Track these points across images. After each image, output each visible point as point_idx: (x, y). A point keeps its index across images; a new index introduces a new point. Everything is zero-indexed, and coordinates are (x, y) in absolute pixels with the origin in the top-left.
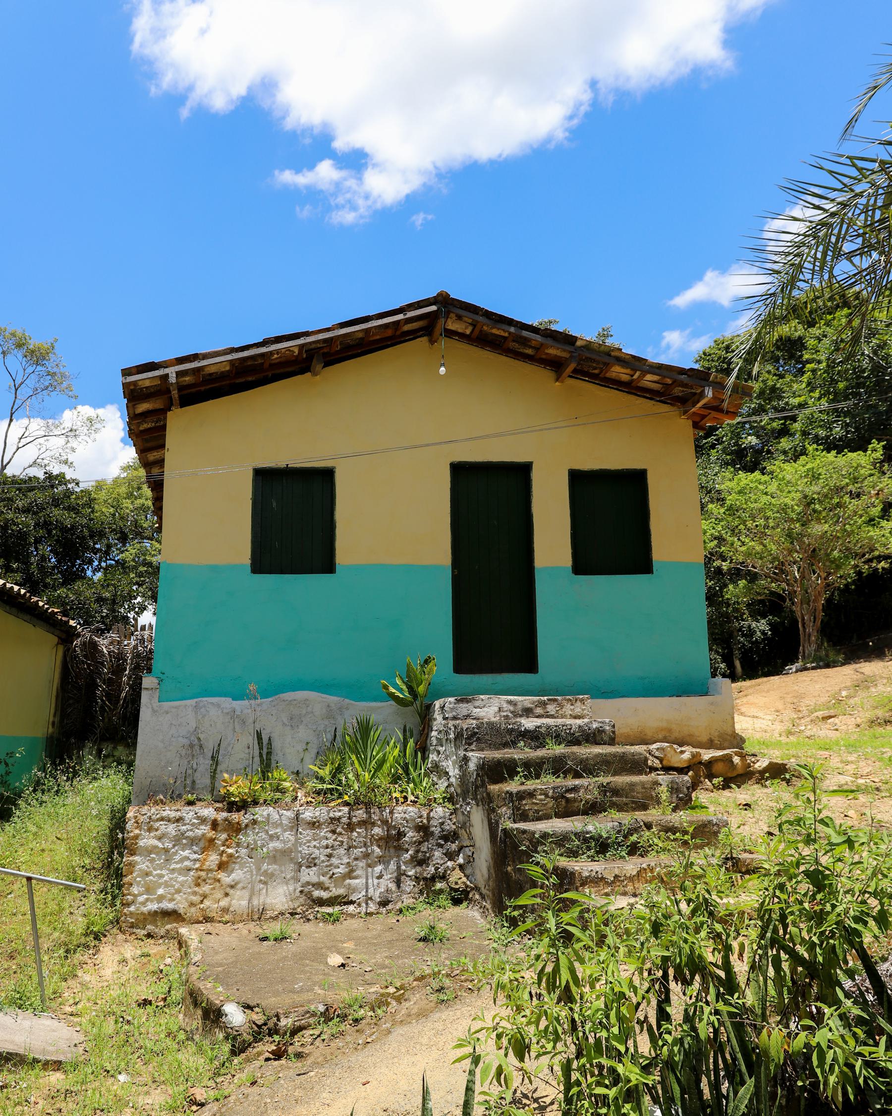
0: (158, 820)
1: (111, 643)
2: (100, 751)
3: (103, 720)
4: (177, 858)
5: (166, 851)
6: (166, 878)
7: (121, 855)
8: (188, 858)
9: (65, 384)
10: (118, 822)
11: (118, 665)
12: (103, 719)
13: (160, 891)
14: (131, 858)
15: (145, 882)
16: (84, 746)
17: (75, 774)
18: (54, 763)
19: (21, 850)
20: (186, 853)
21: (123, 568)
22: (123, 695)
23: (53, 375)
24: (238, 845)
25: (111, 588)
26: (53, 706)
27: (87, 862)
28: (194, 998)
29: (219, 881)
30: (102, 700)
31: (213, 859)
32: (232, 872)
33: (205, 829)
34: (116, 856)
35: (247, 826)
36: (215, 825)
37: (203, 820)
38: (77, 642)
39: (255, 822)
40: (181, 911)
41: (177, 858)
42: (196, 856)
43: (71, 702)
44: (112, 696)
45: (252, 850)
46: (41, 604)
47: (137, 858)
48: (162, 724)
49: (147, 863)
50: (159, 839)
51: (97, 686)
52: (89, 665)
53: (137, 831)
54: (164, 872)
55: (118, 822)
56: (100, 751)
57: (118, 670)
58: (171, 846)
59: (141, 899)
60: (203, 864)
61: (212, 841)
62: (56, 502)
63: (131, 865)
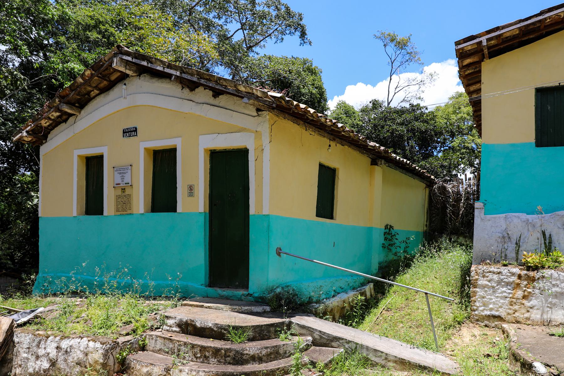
0: (488, 272)
1: (453, 187)
3: (451, 224)
4: (499, 291)
5: (493, 287)
6: (494, 300)
7: (469, 288)
8: (505, 292)
9: (416, 58)
10: (466, 272)
11: (457, 198)
13: (491, 306)
14: (474, 289)
15: (483, 301)
17: (440, 249)
18: (428, 243)
19: (417, 282)
20: (504, 289)
21: (453, 150)
22: (461, 212)
23: (410, 53)
24: (534, 287)
25: (448, 160)
26: (426, 217)
27: (450, 289)
28: (515, 357)
29: (523, 304)
31: (519, 294)
32: (531, 300)
33: (514, 279)
34: (466, 287)
35: (538, 279)
36: (520, 277)
37: (513, 274)
38: (435, 186)
39: (543, 277)
41: (499, 291)
42: (510, 291)
44: (455, 213)
45: (542, 291)
46: (417, 168)
47: (477, 289)
48: (487, 226)
50: (489, 281)
52: (442, 198)
53: (477, 277)
54: (492, 297)
55: (466, 272)
57: (458, 200)
58: (495, 285)
60: (514, 295)
61: (518, 285)
62: (416, 119)
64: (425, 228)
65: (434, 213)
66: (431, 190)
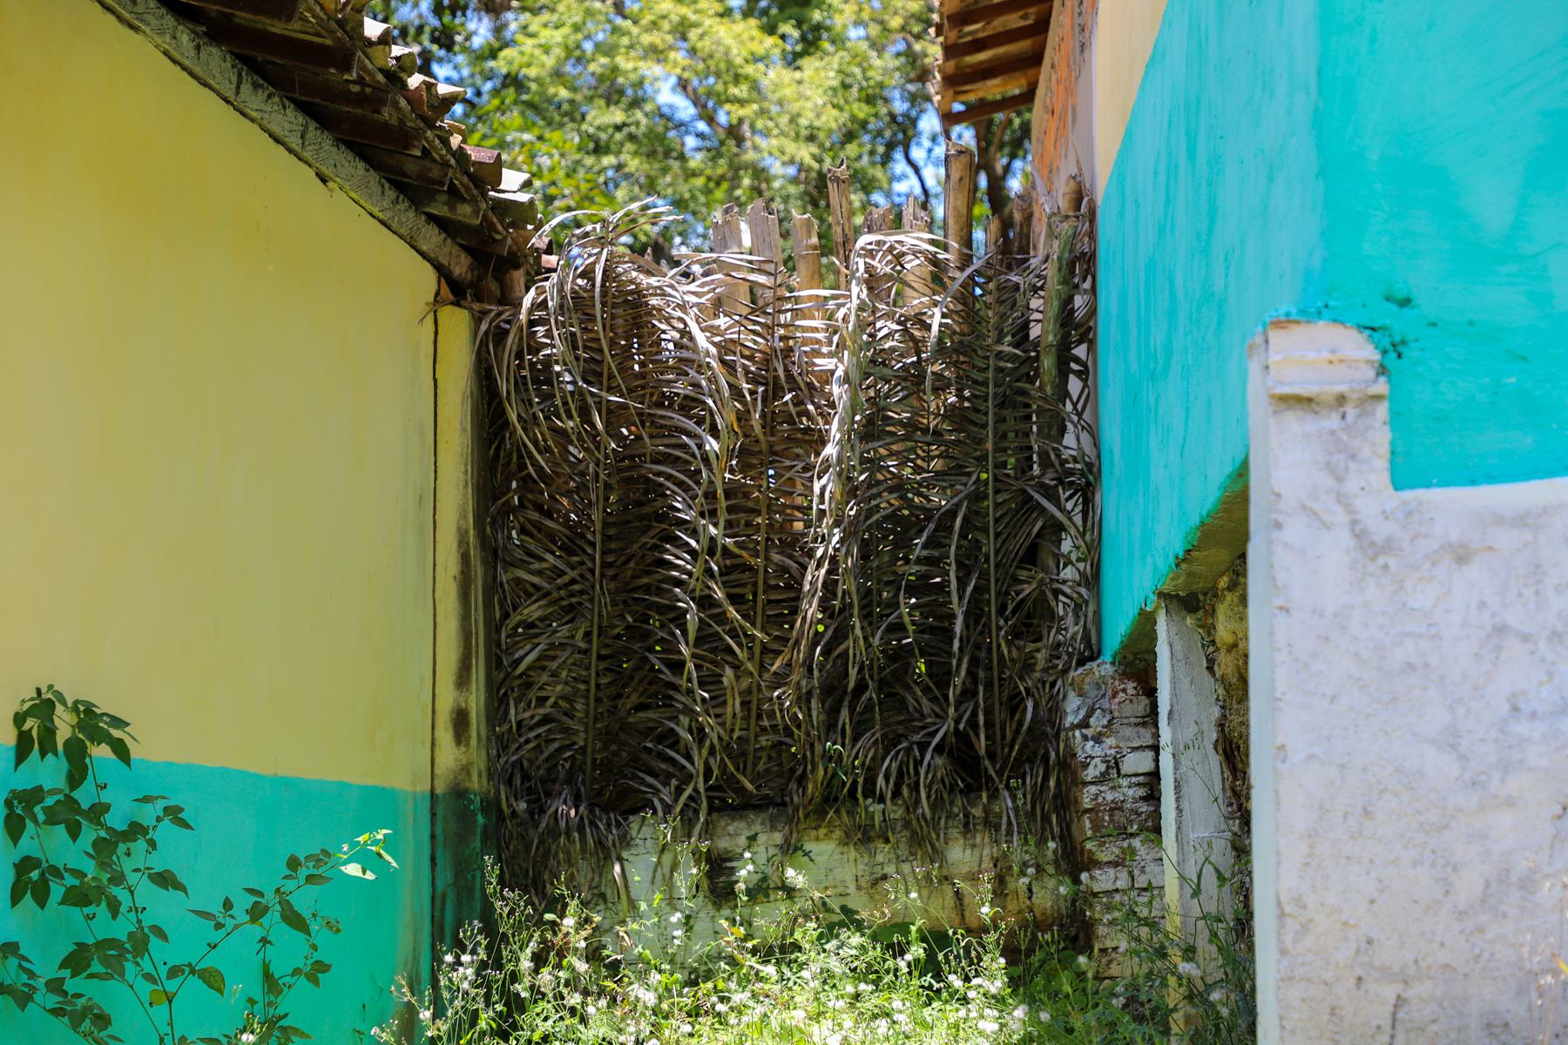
2: (718, 869)
12: (718, 701)
16: (625, 841)
22: (815, 576)
30: (705, 602)
43: (533, 611)
51: (667, 529)
52: (614, 415)
56: (718, 869)
64: (449, 756)
65: (530, 592)
66: (500, 336)
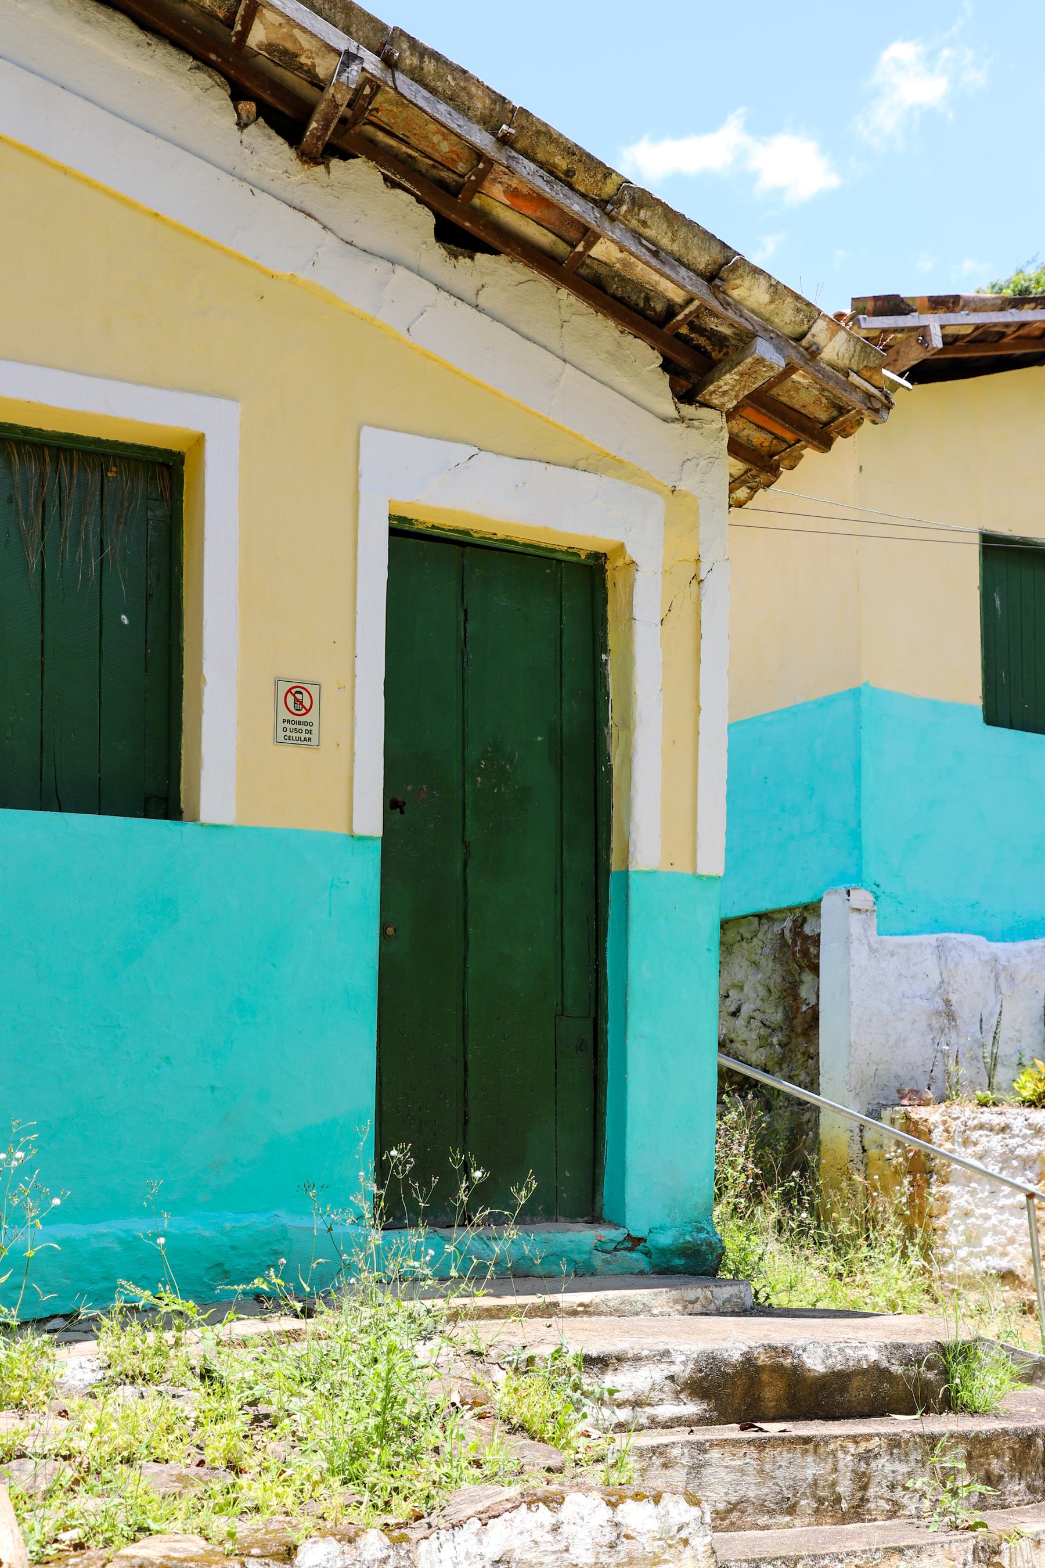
6: (994, 1221)
13: (987, 1241)
14: (944, 1188)
40: (1019, 1272)
49: (967, 1197)
50: (981, 1158)
54: (990, 1211)
59: (962, 1253)
63: (944, 1198)
